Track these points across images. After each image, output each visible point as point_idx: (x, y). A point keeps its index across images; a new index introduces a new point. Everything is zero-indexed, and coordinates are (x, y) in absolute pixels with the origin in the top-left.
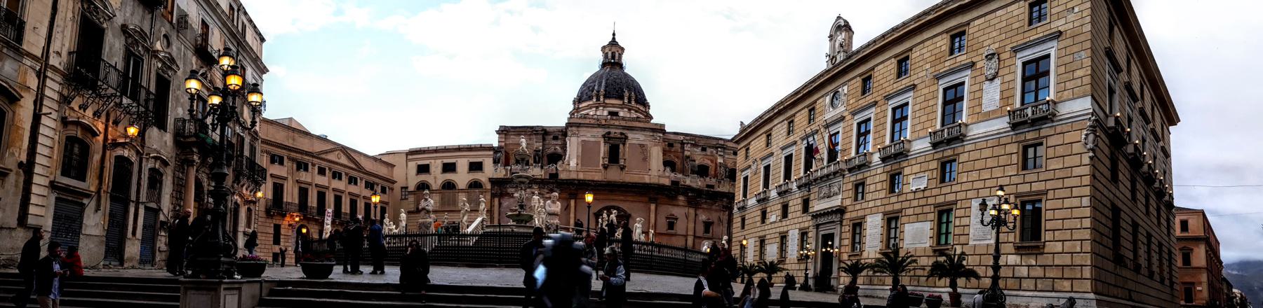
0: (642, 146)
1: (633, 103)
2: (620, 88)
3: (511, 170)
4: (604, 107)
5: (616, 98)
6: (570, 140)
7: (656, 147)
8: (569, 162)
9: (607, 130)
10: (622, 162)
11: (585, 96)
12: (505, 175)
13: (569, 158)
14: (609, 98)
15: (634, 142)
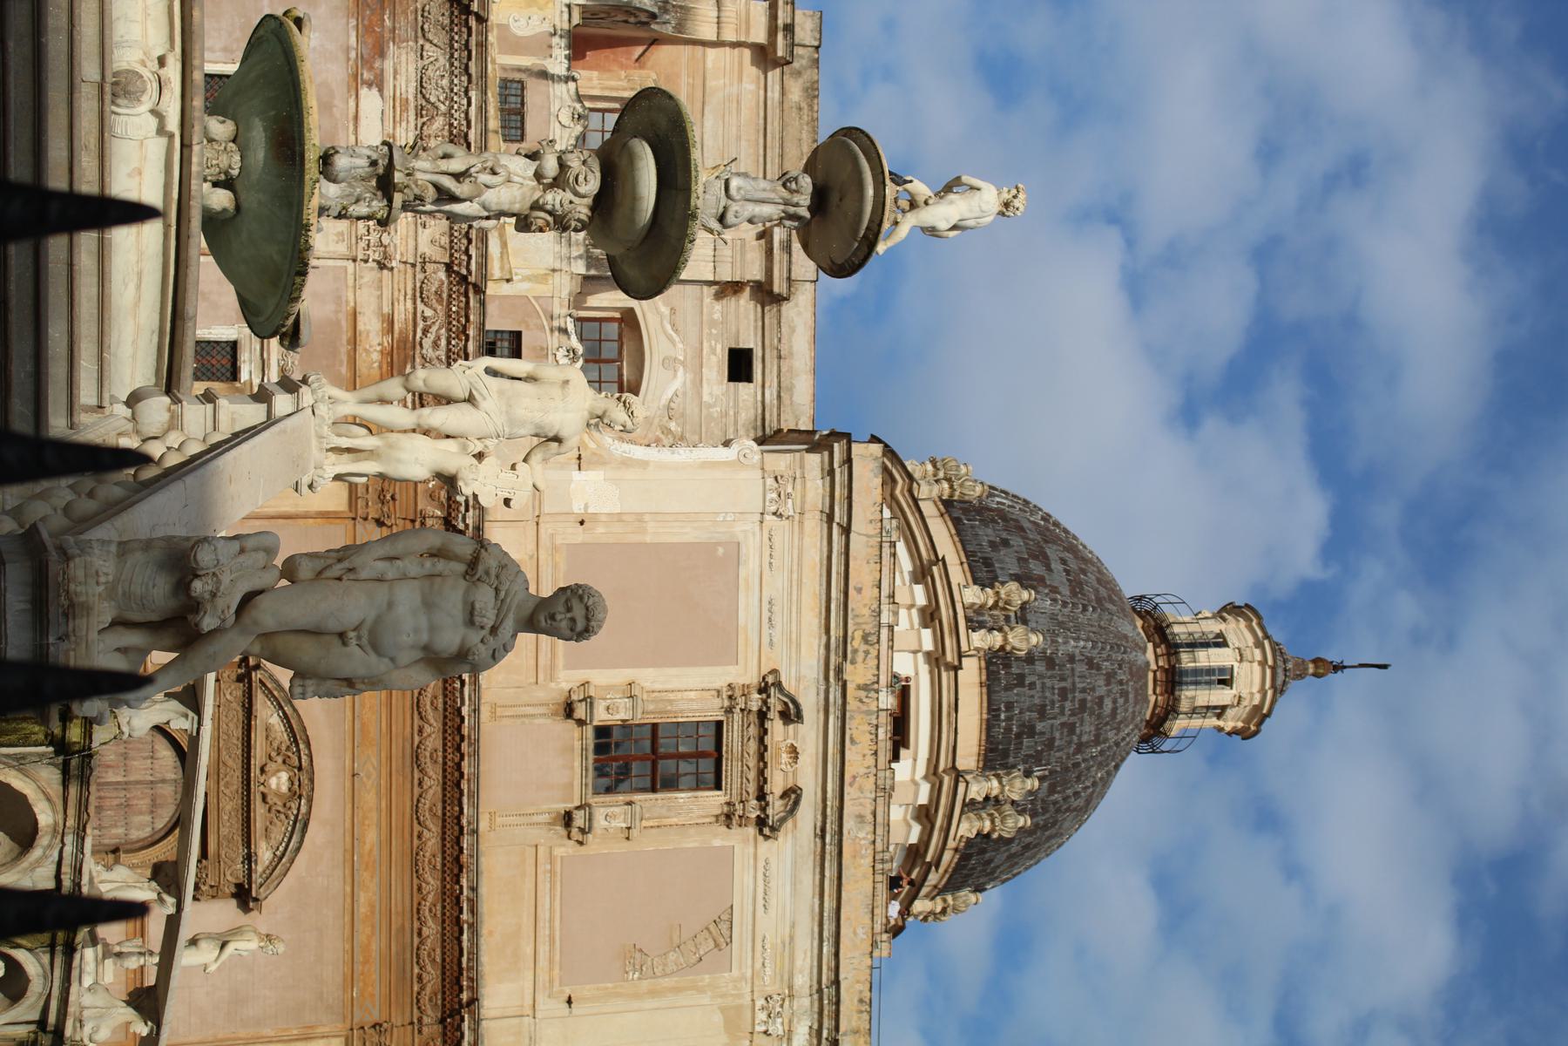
0: (721, 930)
1: (967, 828)
2: (1050, 744)
3: (544, 75)
4: (935, 660)
5: (990, 725)
6: (738, 464)
7: (718, 1018)
8: (600, 461)
9: (809, 703)
10: (610, 814)
11: (987, 534)
12: (504, 28)
13: (627, 463)
14: (991, 683)
15: (744, 879)
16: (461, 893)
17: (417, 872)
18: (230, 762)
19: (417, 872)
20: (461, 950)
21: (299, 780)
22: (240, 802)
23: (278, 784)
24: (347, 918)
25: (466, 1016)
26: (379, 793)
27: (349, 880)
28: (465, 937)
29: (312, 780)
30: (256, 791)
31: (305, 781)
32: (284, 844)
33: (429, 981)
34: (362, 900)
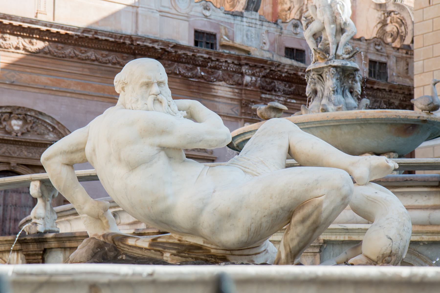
16: (78, 35)
17: (63, 57)
18: (3, 150)
19: (63, 57)
20: (106, 40)
21: (17, 114)
22: (23, 147)
23: (18, 126)
24: (82, 97)
25: (138, 43)
26: (23, 72)
27: (64, 94)
28: (100, 37)
29: (19, 108)
30: (20, 138)
31: (19, 111)
32: (48, 126)
33: (116, 59)
34: (75, 88)
